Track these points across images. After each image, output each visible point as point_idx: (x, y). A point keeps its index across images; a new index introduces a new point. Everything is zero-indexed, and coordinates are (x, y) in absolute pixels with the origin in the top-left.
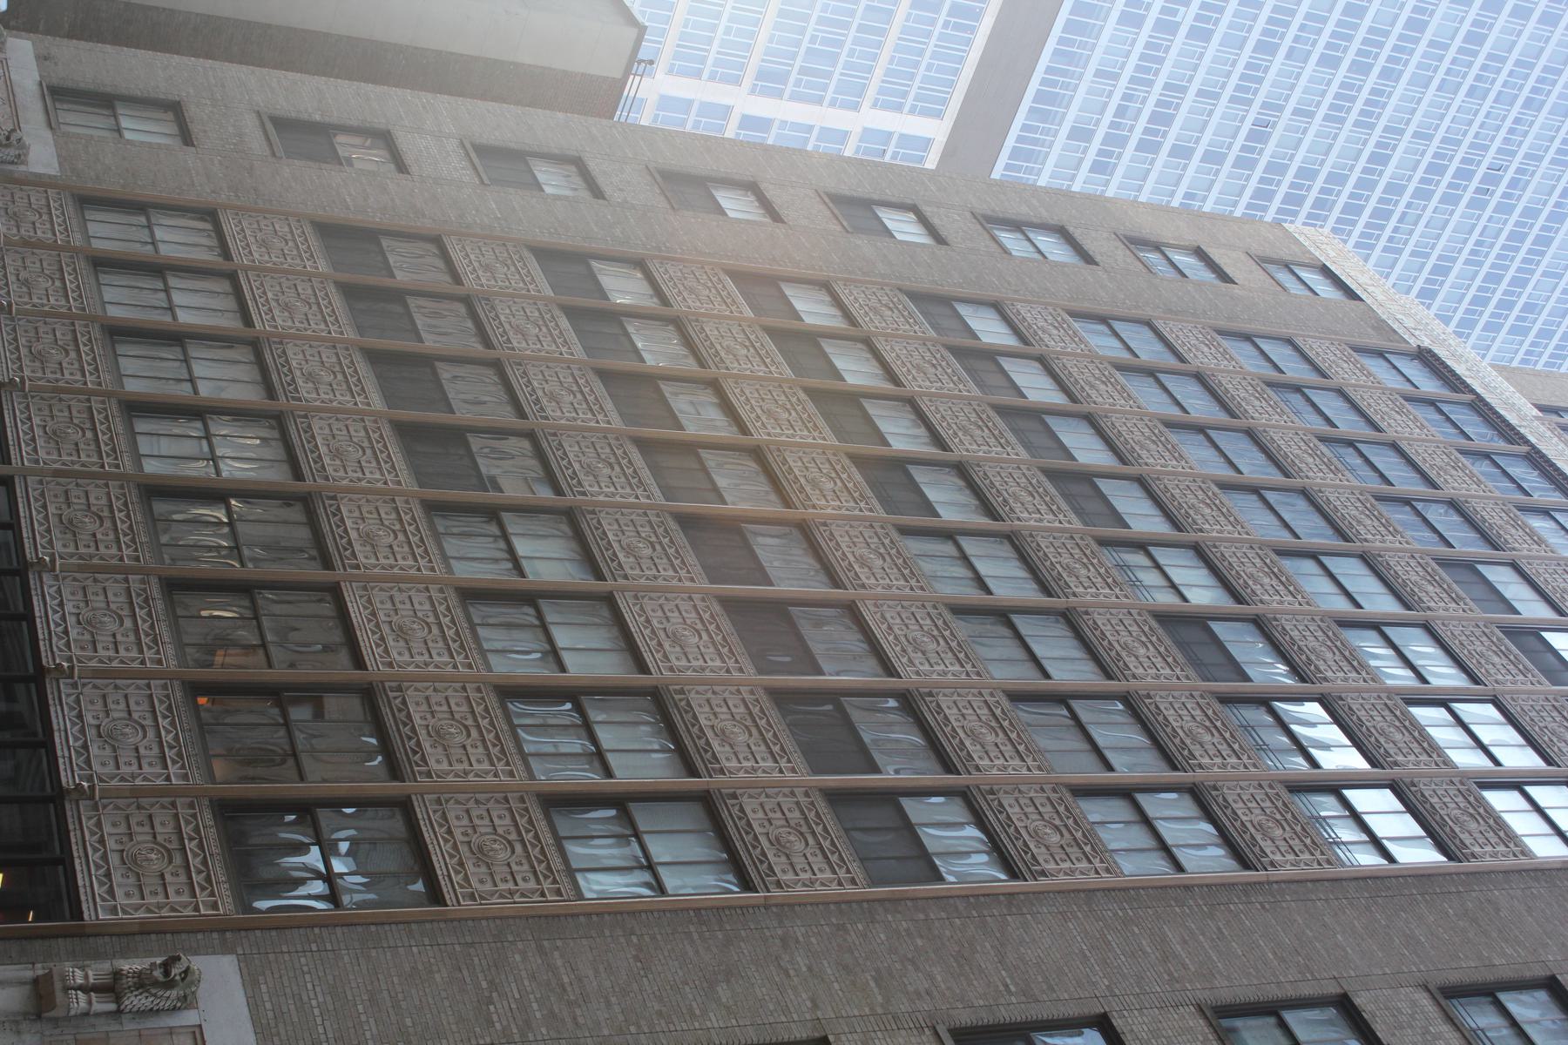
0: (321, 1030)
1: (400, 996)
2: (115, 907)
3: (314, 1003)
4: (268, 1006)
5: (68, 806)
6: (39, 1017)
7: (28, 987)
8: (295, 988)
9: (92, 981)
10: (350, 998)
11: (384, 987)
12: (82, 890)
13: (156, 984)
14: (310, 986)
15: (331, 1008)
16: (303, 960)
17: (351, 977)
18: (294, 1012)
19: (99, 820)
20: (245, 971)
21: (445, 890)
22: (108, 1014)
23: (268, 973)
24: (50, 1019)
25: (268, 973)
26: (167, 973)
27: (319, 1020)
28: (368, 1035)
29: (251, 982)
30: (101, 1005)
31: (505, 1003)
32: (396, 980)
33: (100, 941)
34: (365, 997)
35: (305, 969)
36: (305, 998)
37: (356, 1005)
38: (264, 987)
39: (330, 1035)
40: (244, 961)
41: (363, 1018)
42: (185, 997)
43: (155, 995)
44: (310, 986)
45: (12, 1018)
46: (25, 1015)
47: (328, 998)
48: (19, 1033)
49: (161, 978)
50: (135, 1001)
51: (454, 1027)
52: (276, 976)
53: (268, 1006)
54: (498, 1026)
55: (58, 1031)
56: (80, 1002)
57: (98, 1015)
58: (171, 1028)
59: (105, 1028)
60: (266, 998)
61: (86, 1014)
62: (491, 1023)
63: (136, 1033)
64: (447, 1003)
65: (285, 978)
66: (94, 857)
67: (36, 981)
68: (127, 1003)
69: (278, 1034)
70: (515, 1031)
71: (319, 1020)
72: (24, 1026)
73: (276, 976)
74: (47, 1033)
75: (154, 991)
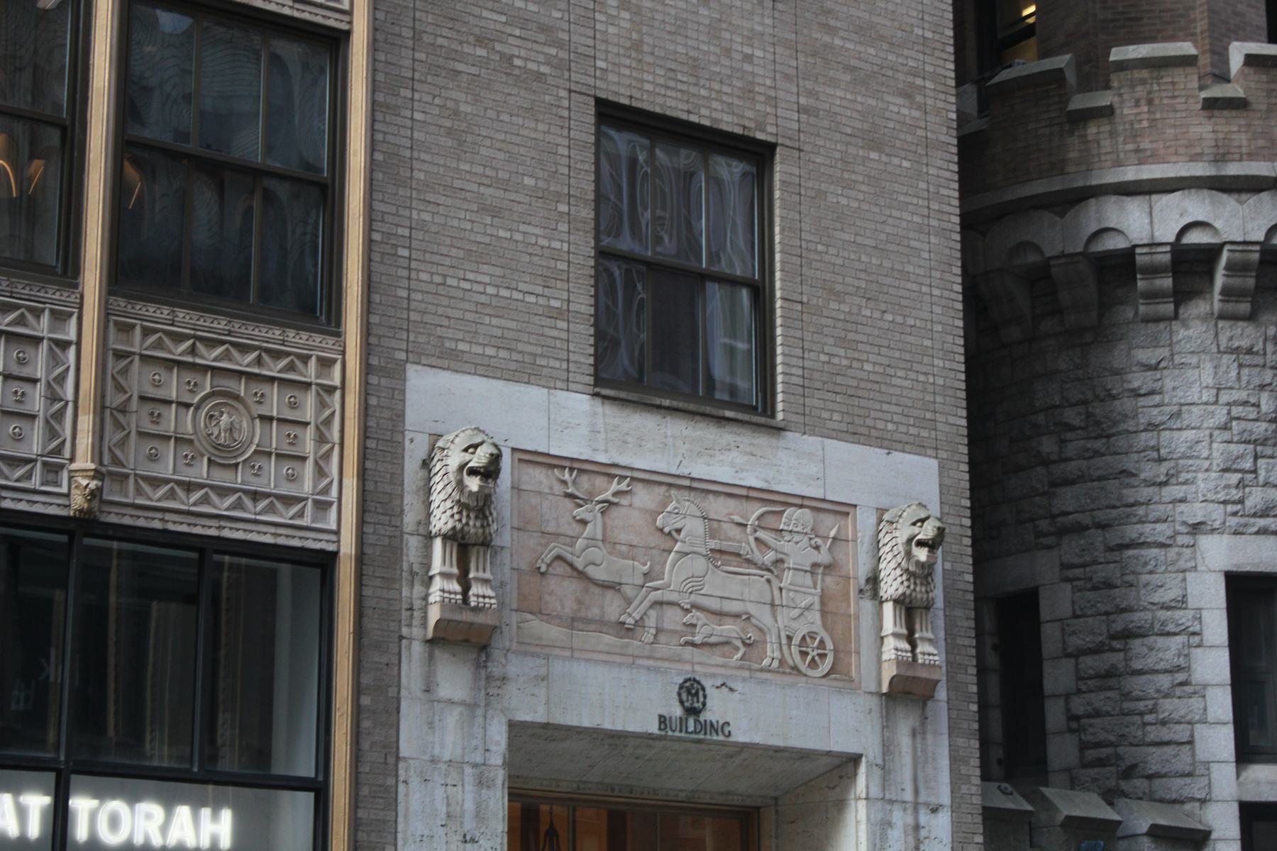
0: (532, 299)
1: (489, 172)
2: (316, 502)
3: (490, 290)
4: (490, 351)
5: (113, 519)
7: (437, 652)
8: (466, 305)
9: (455, 570)
10: (487, 240)
11: (474, 187)
12: (281, 541)
14: (467, 285)
15: (498, 271)
16: (424, 276)
17: (455, 223)
18: (503, 323)
19: (145, 478)
20: (434, 361)
21: (319, 20)
23: (439, 331)
25: (439, 331)
27: (516, 295)
28: (545, 243)
29: (451, 360)
31: (511, 40)
32: (466, 167)
33: (370, 539)
34: (488, 220)
35: (438, 279)
36: (483, 299)
37: (498, 237)
38: (462, 346)
39: (539, 290)
40: (418, 355)
41: (519, 237)
44: (467, 285)
45: (483, 683)
46: (479, 666)
47: (485, 268)
48: (504, 679)
51: (541, 127)
52: (446, 323)
53: (490, 351)
54: (543, 69)
55: (505, 629)
58: (513, 488)
59: (507, 569)
60: (477, 349)
62: (539, 77)
63: (515, 532)
64: (505, 117)
65: (450, 312)
66: (223, 505)
69: (535, 355)
70: (553, 51)
71: (516, 295)
72: (495, 669)
73: (446, 323)
74: (507, 644)
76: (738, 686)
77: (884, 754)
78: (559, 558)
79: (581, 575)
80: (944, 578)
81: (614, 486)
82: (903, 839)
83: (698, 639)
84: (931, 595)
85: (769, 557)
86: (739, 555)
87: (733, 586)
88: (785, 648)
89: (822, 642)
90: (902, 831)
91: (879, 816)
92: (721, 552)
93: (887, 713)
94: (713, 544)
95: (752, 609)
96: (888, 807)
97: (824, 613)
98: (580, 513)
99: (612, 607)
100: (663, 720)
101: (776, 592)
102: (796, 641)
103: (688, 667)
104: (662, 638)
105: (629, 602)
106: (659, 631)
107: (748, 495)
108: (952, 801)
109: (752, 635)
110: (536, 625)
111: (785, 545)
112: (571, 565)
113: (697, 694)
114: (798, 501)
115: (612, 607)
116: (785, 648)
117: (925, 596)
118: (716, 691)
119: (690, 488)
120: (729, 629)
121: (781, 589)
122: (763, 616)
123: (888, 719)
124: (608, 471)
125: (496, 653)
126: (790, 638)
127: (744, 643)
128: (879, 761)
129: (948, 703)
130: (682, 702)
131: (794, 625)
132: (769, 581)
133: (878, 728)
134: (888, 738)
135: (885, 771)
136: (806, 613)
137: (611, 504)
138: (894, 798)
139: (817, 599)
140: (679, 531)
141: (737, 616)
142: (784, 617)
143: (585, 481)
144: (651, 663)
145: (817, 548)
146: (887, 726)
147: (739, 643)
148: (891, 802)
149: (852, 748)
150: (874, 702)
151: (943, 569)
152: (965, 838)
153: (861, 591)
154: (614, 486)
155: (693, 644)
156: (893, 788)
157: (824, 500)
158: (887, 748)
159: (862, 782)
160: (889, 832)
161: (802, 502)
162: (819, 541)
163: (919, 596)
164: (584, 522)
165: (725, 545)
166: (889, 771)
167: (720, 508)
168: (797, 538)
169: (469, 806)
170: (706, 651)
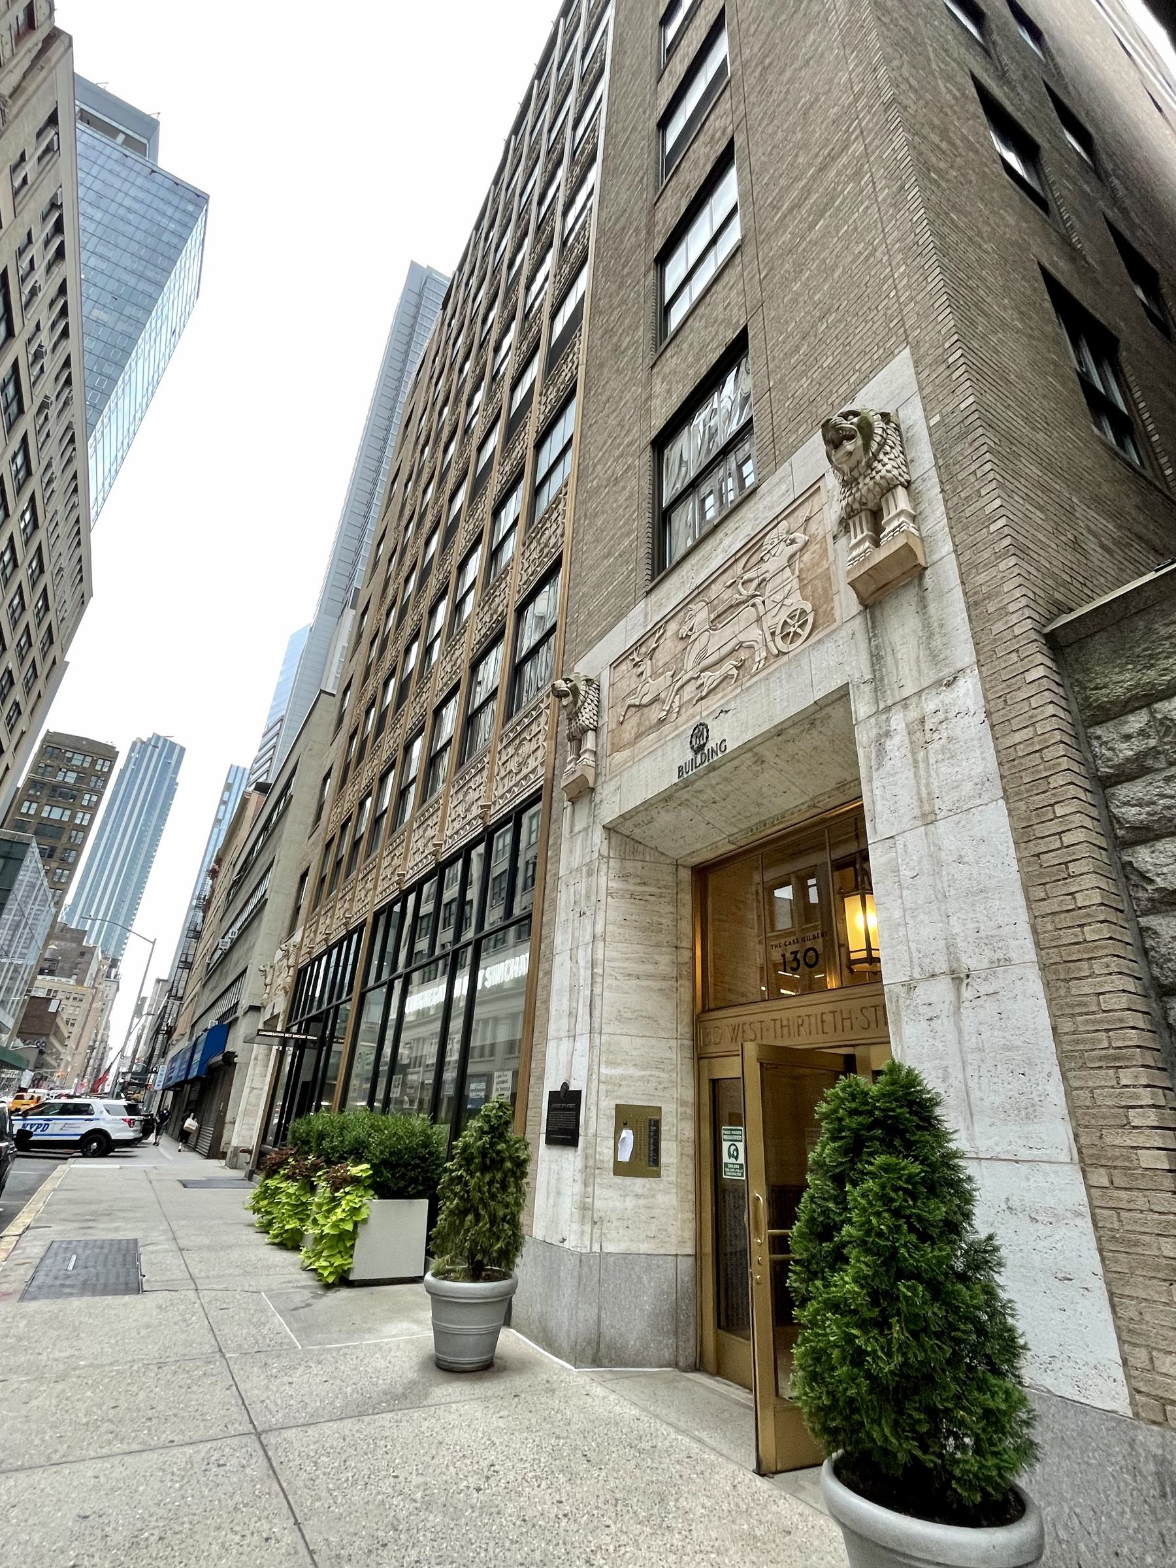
6: (593, 790)
13: (575, 703)
22: (597, 737)
24: (595, 781)
26: (566, 695)
30: (589, 742)
42: (587, 680)
43: (583, 703)
49: (570, 698)
50: (586, 716)
56: (587, 758)
57: (597, 746)
61: (595, 753)
67: (573, 801)
68: (587, 722)
72: (598, 800)
75: (580, 703)
76: (732, 705)
77: (873, 665)
78: (630, 706)
79: (640, 706)
80: (930, 435)
81: (657, 635)
82: (907, 741)
83: (704, 693)
84: (878, 477)
85: (756, 582)
86: (732, 606)
87: (728, 632)
88: (771, 644)
89: (803, 612)
90: (905, 733)
91: (873, 733)
92: (719, 616)
93: (873, 623)
94: (712, 616)
95: (741, 638)
96: (884, 717)
97: (802, 588)
98: (640, 670)
99: (656, 713)
100: (680, 769)
101: (761, 607)
102: (778, 631)
103: (698, 718)
104: (683, 710)
105: (664, 702)
106: (680, 707)
107: (735, 559)
108: (978, 654)
109: (743, 654)
110: (619, 757)
111: (764, 567)
112: (634, 706)
113: (702, 734)
114: (775, 522)
115: (656, 713)
116: (771, 644)
117: (871, 483)
118: (715, 722)
119: (699, 593)
120: (728, 667)
121: (764, 602)
122: (754, 634)
123: (874, 627)
124: (651, 633)
125: (599, 790)
126: (773, 634)
127: (737, 668)
128: (868, 676)
129: (955, 551)
130: (692, 748)
131: (776, 620)
132: (754, 605)
133: (863, 645)
134: (877, 647)
135: (877, 682)
136: (787, 602)
137: (654, 649)
138: (890, 703)
139: (796, 581)
140: (691, 630)
141: (734, 650)
142: (768, 622)
143: (643, 650)
144: (676, 733)
145: (793, 541)
146: (875, 636)
147: (735, 672)
148: (888, 709)
149: (836, 683)
150: (858, 624)
151: (929, 428)
152: (1009, 686)
153: (835, 537)
154: (657, 635)
155: (702, 698)
156: (888, 692)
157: (795, 500)
158: (876, 658)
159: (861, 707)
160: (888, 743)
161: (776, 520)
162: (792, 536)
163: (864, 490)
164: (642, 673)
165: (720, 609)
166: (882, 679)
167: (716, 589)
168: (773, 552)
169: (584, 892)
170: (711, 697)
